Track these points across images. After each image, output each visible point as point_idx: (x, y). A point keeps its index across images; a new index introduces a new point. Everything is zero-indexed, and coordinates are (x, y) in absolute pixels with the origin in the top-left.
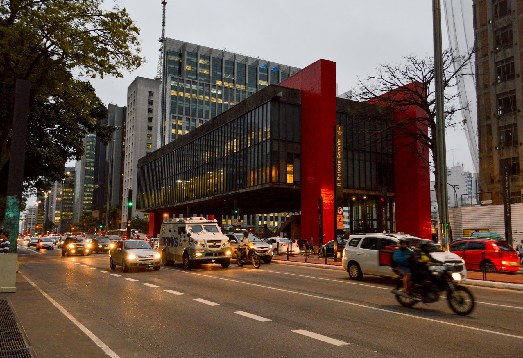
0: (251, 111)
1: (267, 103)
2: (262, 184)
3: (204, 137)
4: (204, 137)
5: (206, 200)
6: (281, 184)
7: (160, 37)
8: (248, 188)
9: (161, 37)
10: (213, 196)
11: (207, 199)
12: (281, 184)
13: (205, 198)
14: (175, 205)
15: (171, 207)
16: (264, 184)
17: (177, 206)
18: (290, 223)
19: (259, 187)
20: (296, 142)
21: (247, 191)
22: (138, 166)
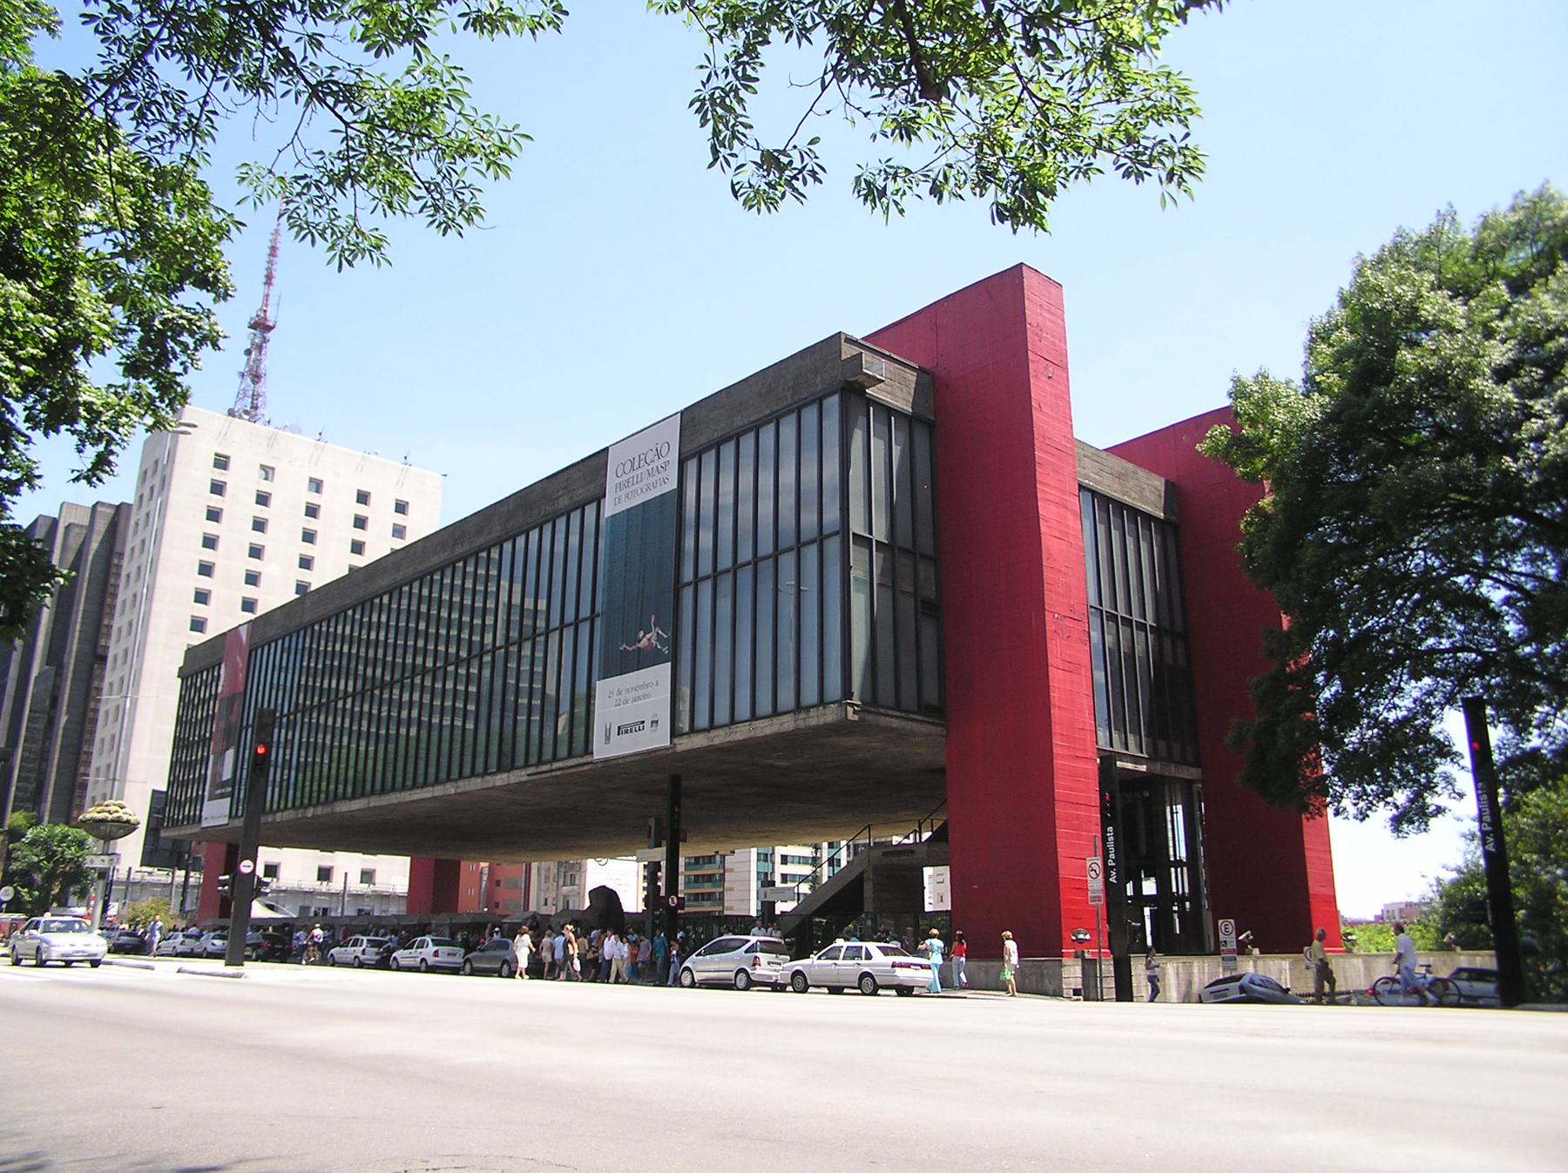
0: (736, 437)
1: (820, 401)
2: (799, 708)
3: (437, 577)
4: (437, 577)
5: (494, 787)
6: (882, 710)
7: (254, 315)
8: (721, 732)
9: (257, 316)
10: (531, 770)
11: (499, 783)
12: (882, 710)
13: (488, 778)
14: (343, 807)
15: (324, 816)
16: (808, 708)
17: (351, 815)
18: (862, 873)
19: (787, 723)
20: (923, 556)
21: (716, 742)
22: (180, 668)
